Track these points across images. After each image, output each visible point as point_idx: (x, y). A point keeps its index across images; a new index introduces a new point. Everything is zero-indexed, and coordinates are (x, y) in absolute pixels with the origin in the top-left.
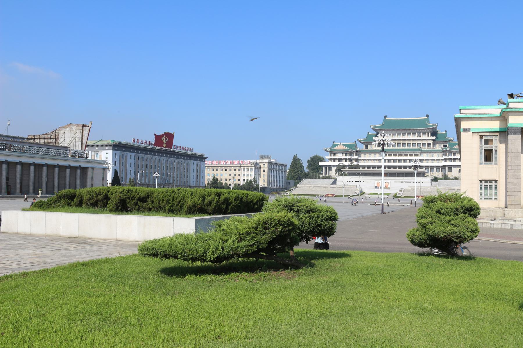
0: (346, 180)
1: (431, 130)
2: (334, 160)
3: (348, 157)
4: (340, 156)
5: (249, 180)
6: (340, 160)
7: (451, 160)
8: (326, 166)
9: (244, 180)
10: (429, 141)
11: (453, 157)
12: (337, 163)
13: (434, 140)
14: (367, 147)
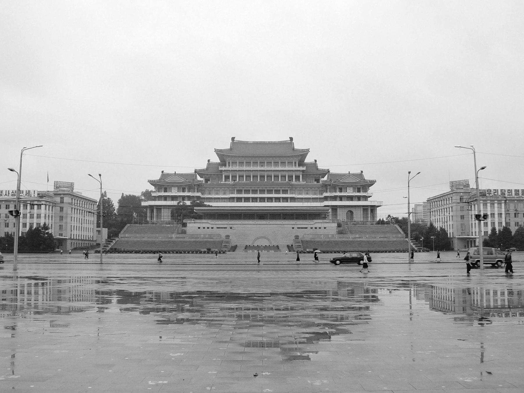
0: (201, 226)
1: (300, 158)
2: (165, 198)
3: (186, 194)
4: (174, 192)
5: (35, 226)
6: (173, 198)
7: (335, 198)
8: (151, 207)
9: (25, 225)
10: (298, 173)
11: (338, 194)
12: (175, 203)
13: (303, 171)
14: (207, 180)
